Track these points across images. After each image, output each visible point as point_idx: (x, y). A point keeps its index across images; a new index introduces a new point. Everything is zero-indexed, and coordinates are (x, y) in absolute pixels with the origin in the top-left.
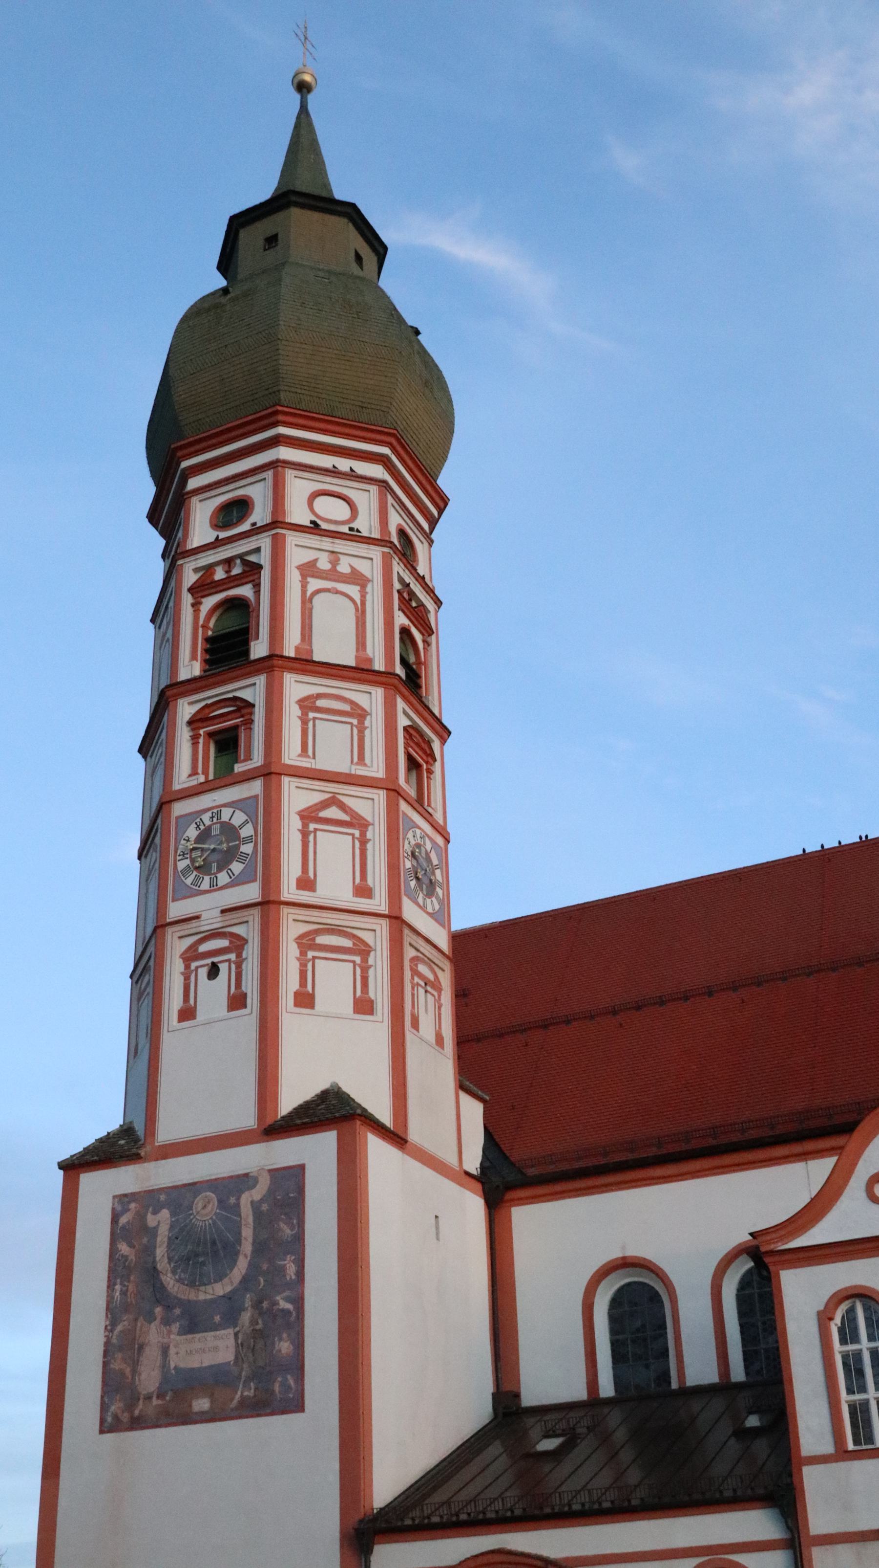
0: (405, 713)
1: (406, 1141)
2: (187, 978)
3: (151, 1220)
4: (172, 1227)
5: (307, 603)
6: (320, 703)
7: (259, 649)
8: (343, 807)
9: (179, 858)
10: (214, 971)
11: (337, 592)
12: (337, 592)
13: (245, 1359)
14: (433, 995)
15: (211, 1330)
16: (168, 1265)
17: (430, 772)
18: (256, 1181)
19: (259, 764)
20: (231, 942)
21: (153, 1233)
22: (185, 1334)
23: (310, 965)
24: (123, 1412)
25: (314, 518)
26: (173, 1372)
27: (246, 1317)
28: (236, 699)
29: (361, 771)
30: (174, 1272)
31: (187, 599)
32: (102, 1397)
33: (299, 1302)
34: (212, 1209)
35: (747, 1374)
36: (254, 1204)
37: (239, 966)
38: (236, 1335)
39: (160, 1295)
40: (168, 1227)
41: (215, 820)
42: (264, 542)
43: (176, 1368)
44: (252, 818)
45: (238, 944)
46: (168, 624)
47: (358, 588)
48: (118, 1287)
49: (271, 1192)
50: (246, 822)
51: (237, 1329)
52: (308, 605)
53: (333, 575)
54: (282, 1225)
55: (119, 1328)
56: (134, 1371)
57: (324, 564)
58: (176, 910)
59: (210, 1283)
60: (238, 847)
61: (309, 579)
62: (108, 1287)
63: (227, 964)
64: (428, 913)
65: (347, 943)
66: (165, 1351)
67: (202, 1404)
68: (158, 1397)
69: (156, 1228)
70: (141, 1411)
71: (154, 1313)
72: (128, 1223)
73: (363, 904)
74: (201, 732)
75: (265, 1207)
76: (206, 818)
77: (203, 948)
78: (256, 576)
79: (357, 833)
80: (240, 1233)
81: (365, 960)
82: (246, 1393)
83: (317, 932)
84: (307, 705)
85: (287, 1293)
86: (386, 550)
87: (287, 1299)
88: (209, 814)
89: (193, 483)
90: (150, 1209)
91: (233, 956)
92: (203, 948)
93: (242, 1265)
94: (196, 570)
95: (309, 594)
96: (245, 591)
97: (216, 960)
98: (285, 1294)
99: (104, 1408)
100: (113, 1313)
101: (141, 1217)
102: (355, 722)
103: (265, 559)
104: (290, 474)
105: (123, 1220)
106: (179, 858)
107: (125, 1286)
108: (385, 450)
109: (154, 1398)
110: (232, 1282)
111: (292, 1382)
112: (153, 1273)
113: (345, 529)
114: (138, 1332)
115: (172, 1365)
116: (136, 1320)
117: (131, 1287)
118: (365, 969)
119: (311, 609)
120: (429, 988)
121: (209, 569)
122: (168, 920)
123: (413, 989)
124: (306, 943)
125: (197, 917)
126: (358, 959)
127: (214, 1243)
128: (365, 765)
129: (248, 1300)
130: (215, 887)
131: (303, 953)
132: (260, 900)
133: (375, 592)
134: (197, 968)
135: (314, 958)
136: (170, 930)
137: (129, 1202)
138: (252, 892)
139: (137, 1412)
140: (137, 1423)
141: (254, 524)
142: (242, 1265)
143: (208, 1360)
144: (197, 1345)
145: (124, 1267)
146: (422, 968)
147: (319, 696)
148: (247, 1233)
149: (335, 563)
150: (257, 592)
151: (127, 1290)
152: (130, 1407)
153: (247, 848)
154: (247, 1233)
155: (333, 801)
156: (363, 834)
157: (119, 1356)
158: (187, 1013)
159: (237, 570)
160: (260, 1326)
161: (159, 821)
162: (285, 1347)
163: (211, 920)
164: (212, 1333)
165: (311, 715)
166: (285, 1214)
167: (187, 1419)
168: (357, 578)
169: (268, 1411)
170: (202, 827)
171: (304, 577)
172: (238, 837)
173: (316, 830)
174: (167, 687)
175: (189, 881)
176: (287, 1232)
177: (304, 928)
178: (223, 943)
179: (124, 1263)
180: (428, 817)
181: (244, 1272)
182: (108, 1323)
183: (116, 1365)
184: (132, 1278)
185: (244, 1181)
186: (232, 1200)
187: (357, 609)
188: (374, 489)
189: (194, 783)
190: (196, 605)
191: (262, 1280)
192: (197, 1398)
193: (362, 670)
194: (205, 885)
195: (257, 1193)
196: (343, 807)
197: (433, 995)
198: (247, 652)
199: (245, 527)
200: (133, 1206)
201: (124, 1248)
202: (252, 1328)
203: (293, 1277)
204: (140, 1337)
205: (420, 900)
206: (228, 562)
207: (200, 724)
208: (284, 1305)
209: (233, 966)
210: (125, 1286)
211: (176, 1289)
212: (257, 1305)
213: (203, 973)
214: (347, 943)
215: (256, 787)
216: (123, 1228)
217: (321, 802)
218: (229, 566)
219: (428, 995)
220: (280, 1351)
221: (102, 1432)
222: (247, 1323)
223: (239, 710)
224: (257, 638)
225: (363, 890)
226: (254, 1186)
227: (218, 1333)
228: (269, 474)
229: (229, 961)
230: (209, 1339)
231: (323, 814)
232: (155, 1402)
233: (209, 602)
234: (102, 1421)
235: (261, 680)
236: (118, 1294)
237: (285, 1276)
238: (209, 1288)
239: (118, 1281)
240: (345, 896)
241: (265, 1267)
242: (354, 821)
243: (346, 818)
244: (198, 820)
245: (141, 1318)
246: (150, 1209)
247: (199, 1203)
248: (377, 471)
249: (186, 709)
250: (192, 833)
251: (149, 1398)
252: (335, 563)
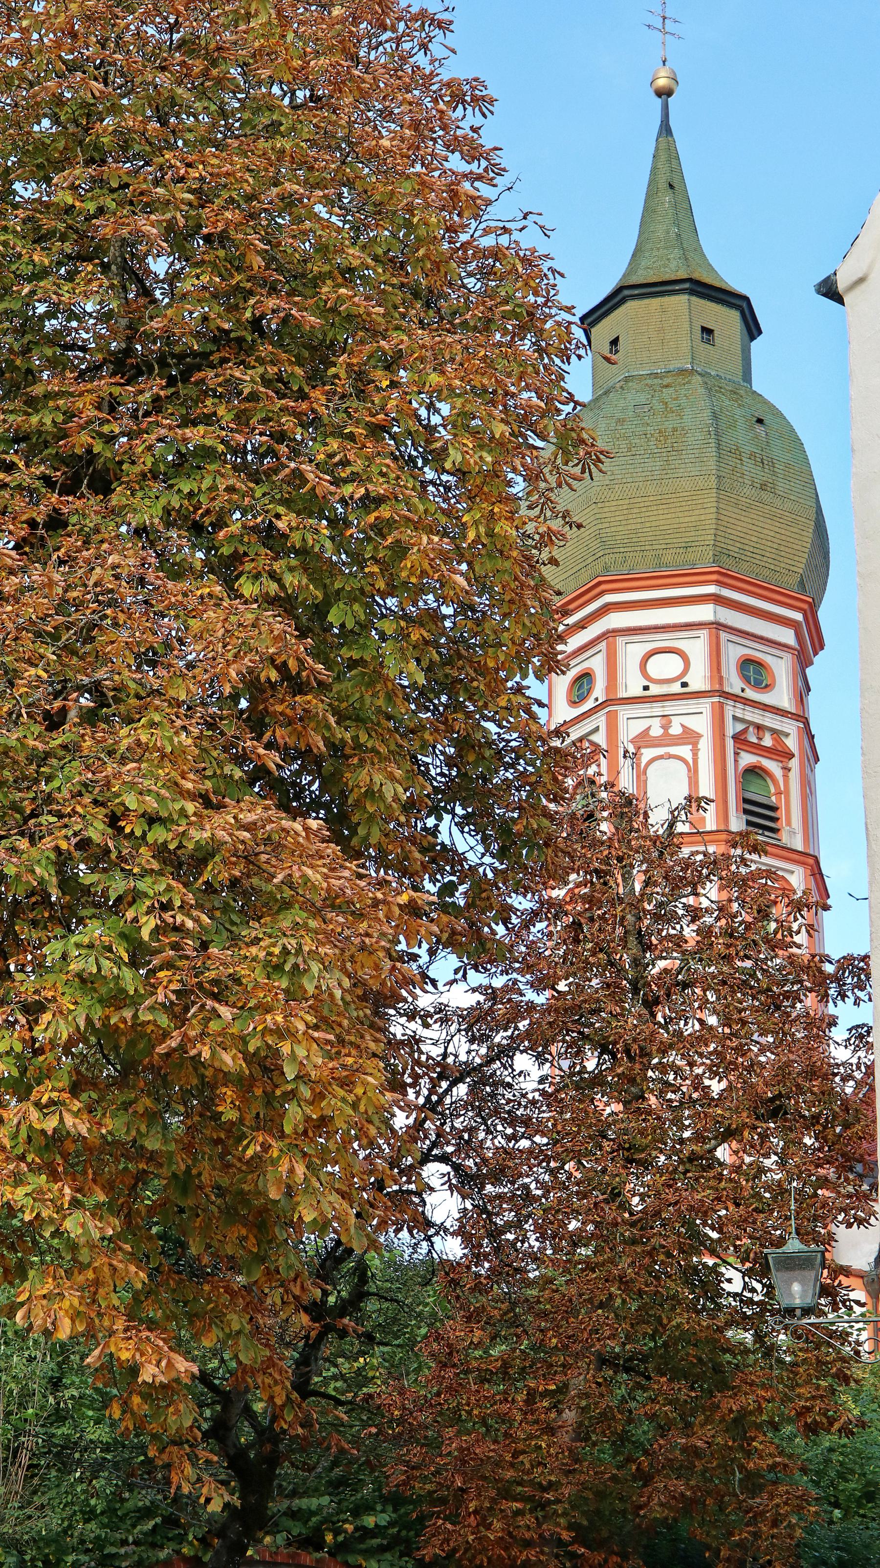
11: (670, 756)
12: (670, 756)
25: (647, 683)
52: (642, 778)
53: (667, 740)
57: (656, 731)
86: (716, 699)
108: (711, 589)
113: (676, 688)
119: (646, 781)
133: (705, 746)
149: (666, 727)
168: (690, 737)
188: (704, 634)
199: (589, 704)
228: (603, 645)
248: (705, 612)
252: (666, 727)
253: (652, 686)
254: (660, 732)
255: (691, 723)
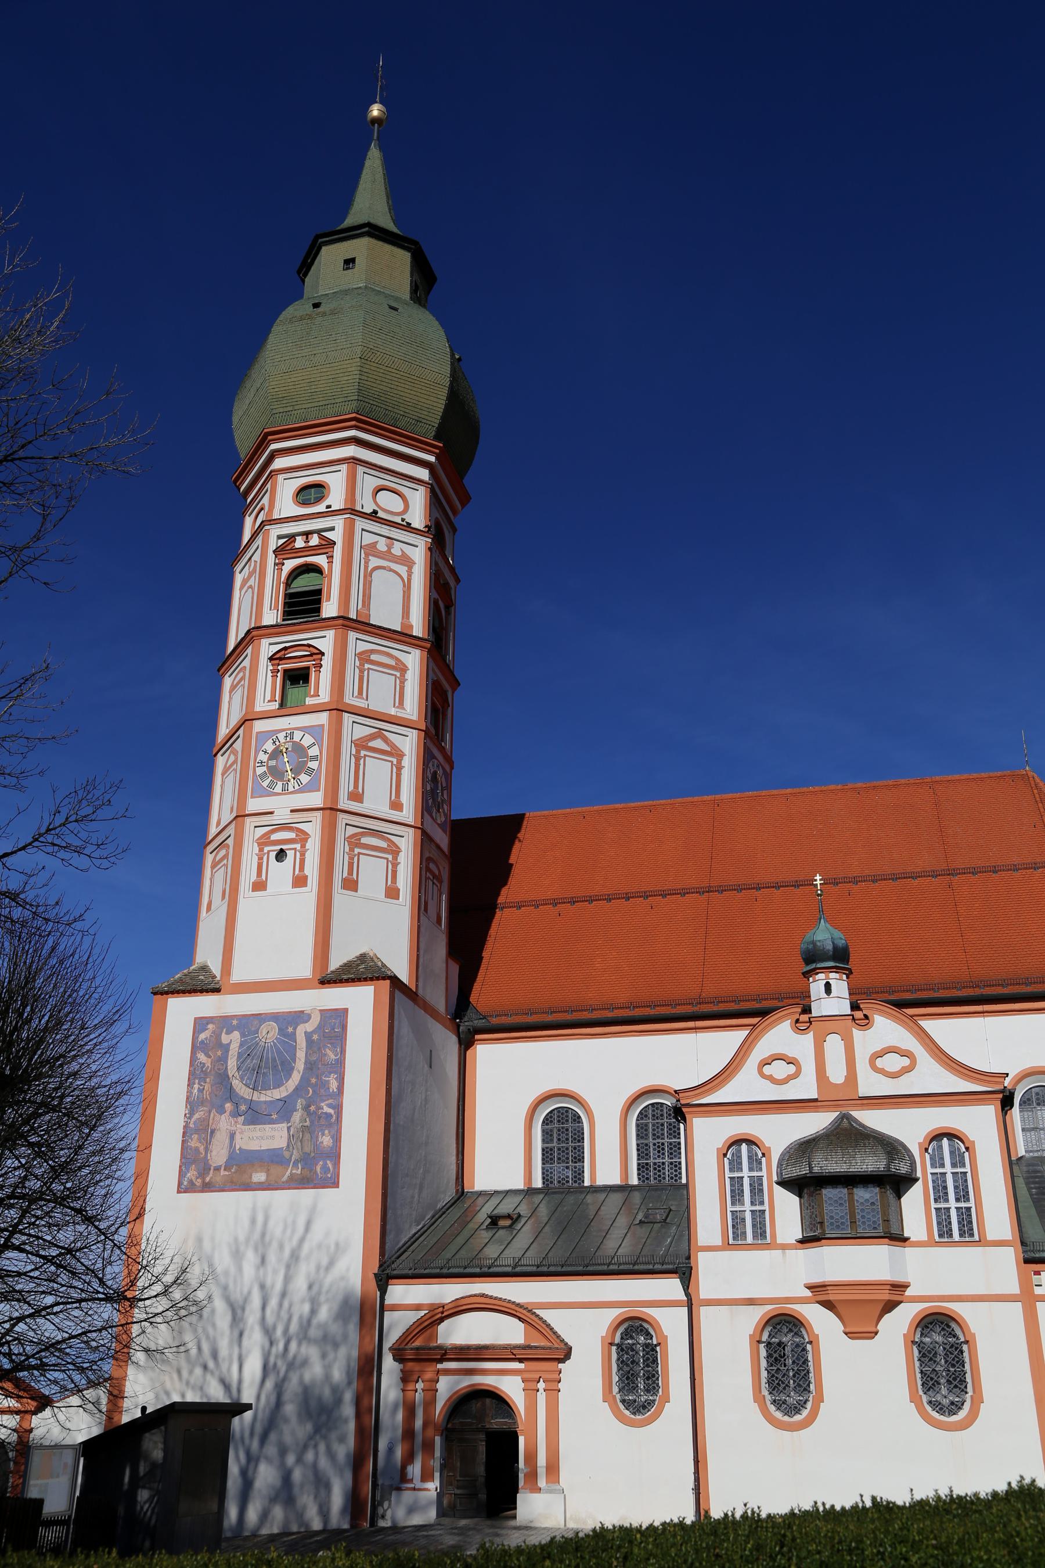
0: (433, 670)
1: (418, 995)
2: (260, 859)
3: (225, 1039)
4: (241, 1045)
5: (368, 576)
6: (373, 657)
7: (330, 609)
8: (386, 740)
9: (257, 765)
10: (281, 855)
11: (391, 570)
12: (391, 570)
13: (295, 1146)
14: (437, 886)
15: (270, 1123)
16: (237, 1073)
17: (445, 715)
18: (309, 1017)
19: (327, 700)
20: (297, 835)
21: (226, 1048)
22: (249, 1125)
23: (356, 859)
24: (197, 1178)
25: (376, 509)
26: (238, 1152)
27: (297, 1117)
28: (309, 646)
29: (401, 714)
30: (242, 1079)
31: (271, 558)
32: (180, 1167)
33: (339, 1108)
34: (274, 1035)
35: (639, 1179)
36: (308, 1036)
37: (303, 854)
38: (289, 1128)
39: (231, 1094)
40: (238, 1044)
41: (288, 739)
42: (338, 522)
43: (240, 1149)
44: (318, 742)
45: (303, 837)
46: (250, 575)
47: (406, 568)
48: (196, 1086)
49: (320, 1027)
50: (313, 744)
51: (289, 1124)
53: (388, 555)
54: (328, 1051)
55: (196, 1116)
56: (207, 1149)
58: (254, 805)
59: (270, 1089)
60: (306, 762)
61: (370, 557)
62: (188, 1085)
63: (293, 851)
64: (438, 824)
65: (383, 844)
66: (232, 1136)
67: (259, 1177)
68: (225, 1170)
69: (229, 1045)
70: (211, 1178)
71: (224, 1108)
72: (206, 1039)
73: (395, 815)
74: (280, 667)
75: (315, 1037)
76: (281, 736)
77: (275, 837)
78: (331, 549)
79: (395, 761)
80: (295, 1055)
81: (395, 858)
82: (294, 1172)
83: (362, 834)
84: (364, 657)
85: (330, 1101)
87: (330, 1106)
88: (284, 733)
89: (279, 463)
90: (225, 1030)
91: (298, 846)
92: (275, 837)
93: (295, 1078)
94: (279, 537)
95: (369, 569)
96: (321, 560)
97: (284, 847)
98: (327, 1102)
99: (181, 1174)
100: (192, 1105)
101: (217, 1035)
102: (398, 674)
103: (337, 536)
104: (360, 469)
105: (202, 1036)
106: (257, 765)
107: (201, 1085)
108: (432, 459)
109: (223, 1168)
110: (287, 1090)
111: (330, 1166)
112: (223, 1078)
113: (398, 520)
114: (211, 1121)
115: (237, 1147)
116: (210, 1112)
117: (207, 1087)
118: (395, 865)
119: (371, 582)
120: (435, 881)
121: (292, 537)
122: (247, 812)
123: (426, 882)
124: (354, 842)
125: (272, 813)
126: (390, 857)
127: (274, 1060)
128: (404, 709)
129: (300, 1103)
130: (285, 791)
131: (352, 850)
132: (322, 806)
134: (269, 852)
135: (359, 854)
136: (248, 820)
137: (207, 1024)
138: (316, 799)
139: (208, 1179)
140: (207, 1187)
141: (329, 507)
142: (295, 1078)
143: (265, 1145)
144: (259, 1134)
145: (202, 1071)
146: (432, 866)
147: (372, 651)
148: (301, 1055)
150: (330, 563)
151: (204, 1089)
152: (202, 1174)
153: (313, 765)
154: (301, 1055)
155: (379, 734)
156: (399, 762)
157: (195, 1137)
158: (259, 886)
159: (315, 540)
160: (308, 1123)
161: (241, 732)
162: (326, 1140)
163: (282, 816)
164: (270, 1126)
165: (367, 666)
166: (331, 1044)
167: (248, 1187)
169: (310, 1186)
170: (277, 743)
171: (367, 555)
172: (307, 756)
173: (365, 756)
174: (253, 628)
175: (265, 784)
176: (332, 1056)
177: (351, 831)
178: (291, 835)
179: (202, 1068)
180: (442, 750)
181: (297, 1083)
182: (187, 1112)
183: (194, 1143)
184: (208, 1080)
185: (299, 1017)
186: (290, 1030)
187: (404, 586)
189: (273, 708)
190: (279, 565)
191: (311, 1091)
192: (257, 1172)
193: (406, 634)
194: (278, 788)
195: (309, 1027)
196: (386, 740)
197: (437, 886)
198: (318, 610)
199: (321, 508)
200: (210, 1026)
201: (202, 1057)
202: (301, 1124)
203: (335, 1090)
204: (212, 1124)
205: (434, 814)
206: (307, 534)
207: (277, 662)
208: (327, 1110)
209: (298, 854)
210: (201, 1085)
211: (243, 1091)
212: (306, 1108)
213: (273, 855)
214: (383, 844)
215: (323, 718)
216: (202, 1042)
217: (370, 735)
218: (307, 538)
219: (434, 886)
220: (322, 1143)
221: (179, 1192)
222: (297, 1121)
223: (311, 655)
224: (328, 599)
225: (396, 805)
226: (307, 1022)
227: (274, 1126)
228: (344, 467)
229: (295, 849)
230: (267, 1129)
231: (370, 744)
232: (223, 1172)
233: (290, 565)
234: (180, 1184)
235: (330, 634)
236: (196, 1091)
237: (329, 1088)
238: (269, 1092)
239: (197, 1081)
240: (383, 809)
241: (313, 1080)
242: (393, 751)
243: (388, 748)
244: (275, 737)
245: (214, 1111)
246: (225, 1030)
247: (263, 1030)
248: (424, 474)
249: (267, 647)
250: (269, 747)
251: (217, 1169)
253: (380, 512)
254: (385, 549)
255: (408, 550)
